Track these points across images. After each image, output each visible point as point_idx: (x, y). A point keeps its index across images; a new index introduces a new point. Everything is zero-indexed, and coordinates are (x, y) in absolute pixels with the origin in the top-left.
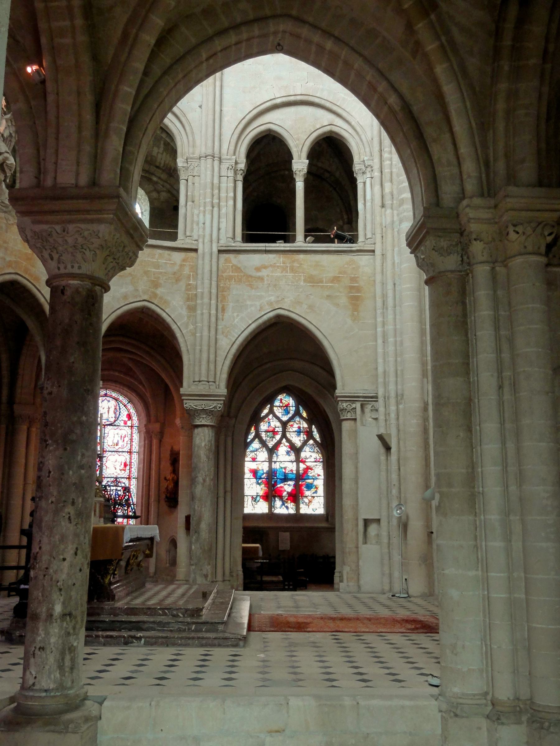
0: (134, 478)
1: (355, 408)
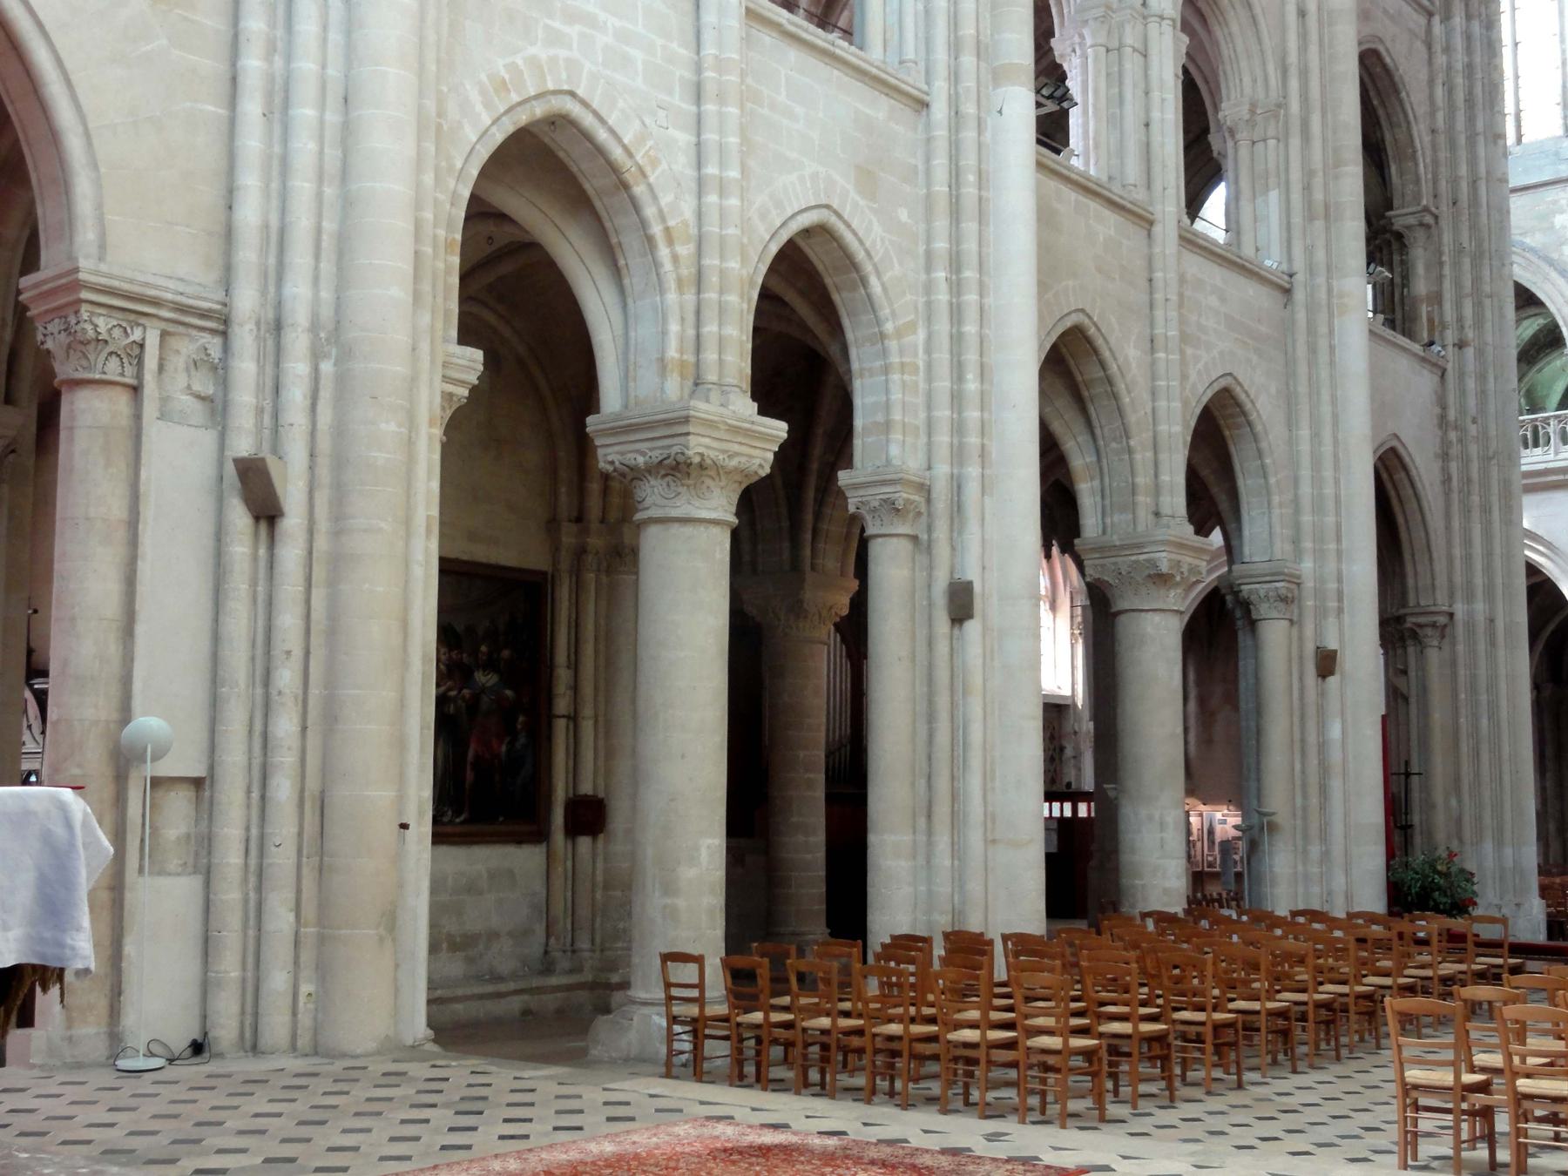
1: (142, 346)
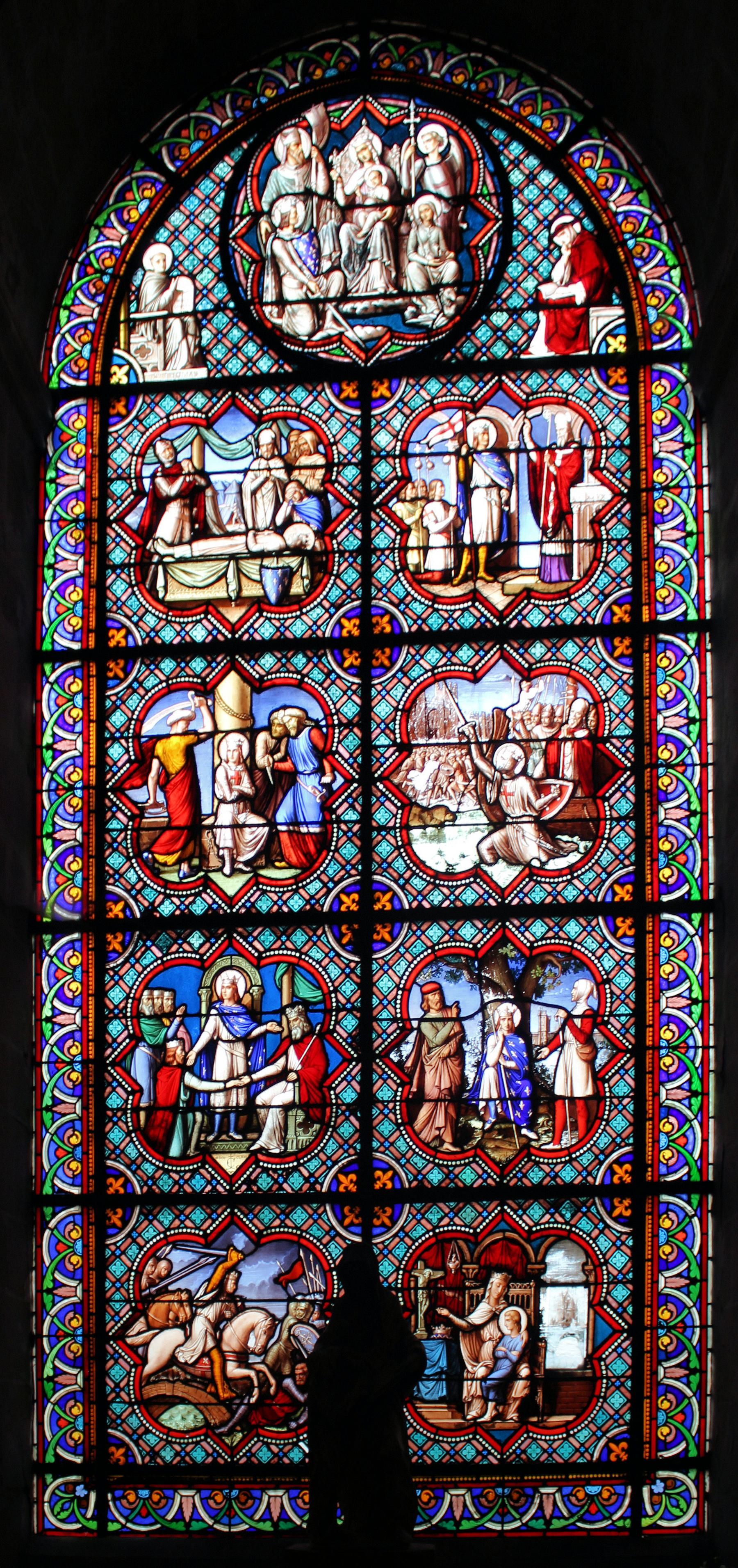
0: (683, 907)
